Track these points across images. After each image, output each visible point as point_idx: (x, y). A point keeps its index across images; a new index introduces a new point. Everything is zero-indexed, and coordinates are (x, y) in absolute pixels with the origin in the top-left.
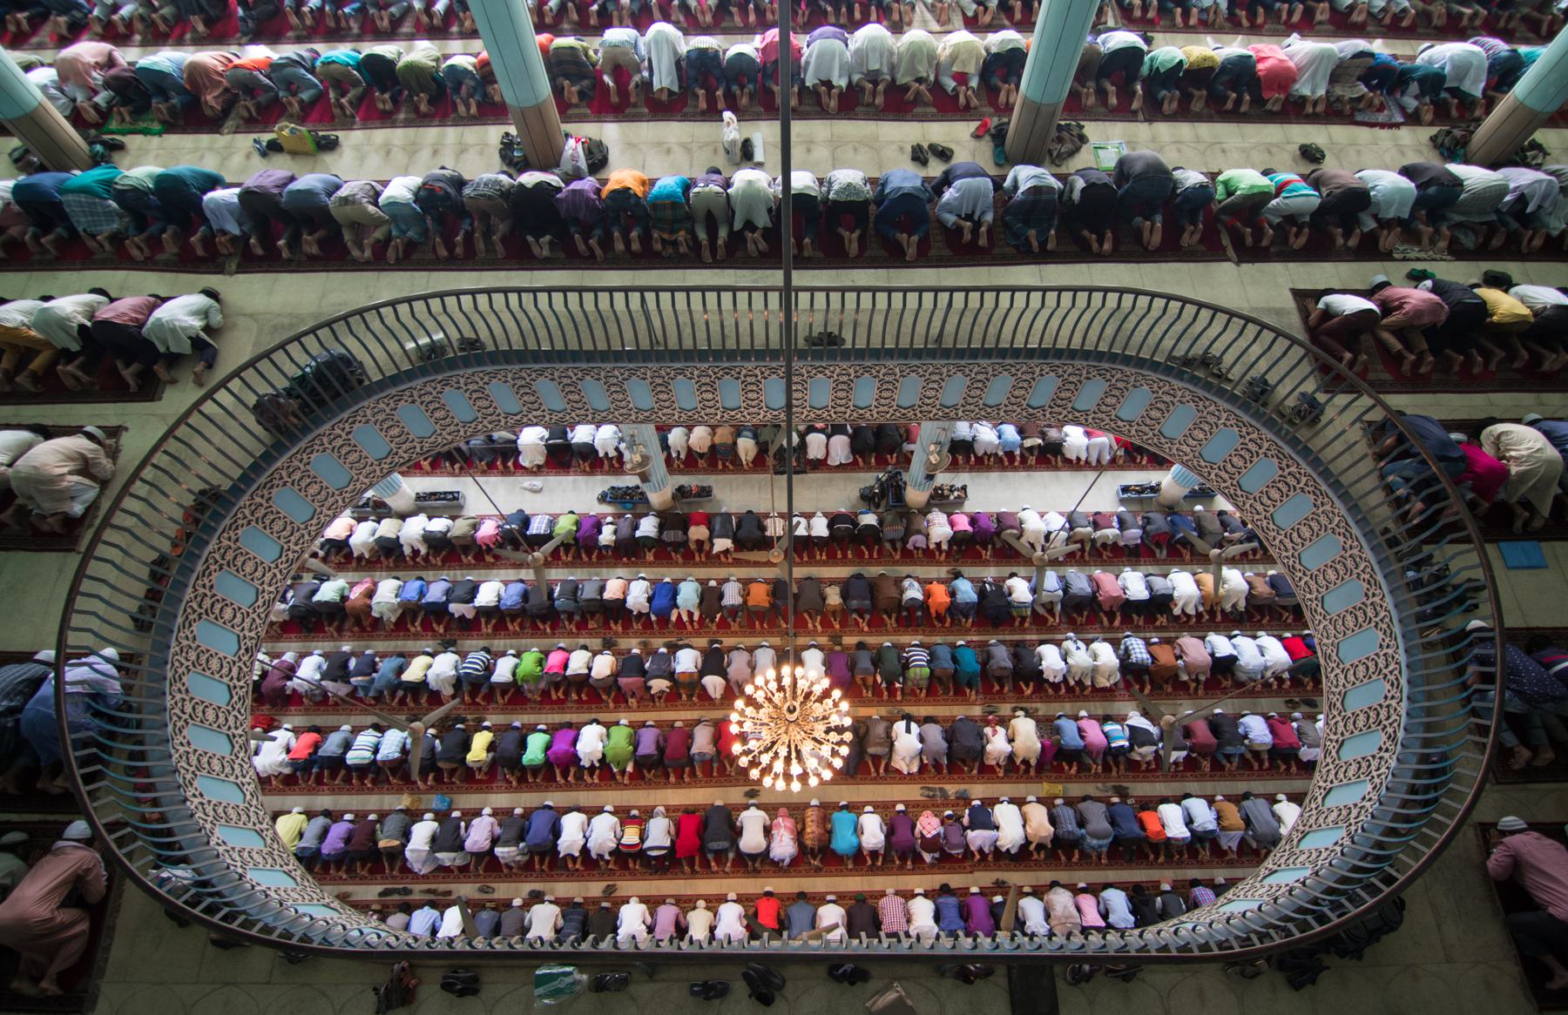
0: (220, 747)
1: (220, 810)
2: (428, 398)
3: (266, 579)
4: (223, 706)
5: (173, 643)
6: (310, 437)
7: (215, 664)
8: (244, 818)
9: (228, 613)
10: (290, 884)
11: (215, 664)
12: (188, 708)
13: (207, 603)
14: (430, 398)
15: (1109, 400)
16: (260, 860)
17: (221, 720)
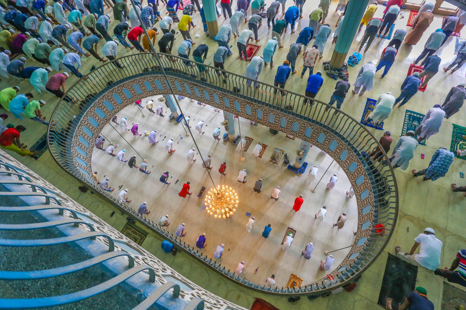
0: (90, 134)
1: (80, 145)
2: (162, 80)
3: (117, 106)
4: (95, 127)
5: (89, 108)
6: (134, 79)
7: (97, 118)
8: (85, 149)
9: (105, 109)
10: (85, 165)
11: (97, 118)
12: (86, 123)
13: (101, 105)
14: (162, 80)
15: (326, 142)
16: (82, 158)
17: (93, 129)
